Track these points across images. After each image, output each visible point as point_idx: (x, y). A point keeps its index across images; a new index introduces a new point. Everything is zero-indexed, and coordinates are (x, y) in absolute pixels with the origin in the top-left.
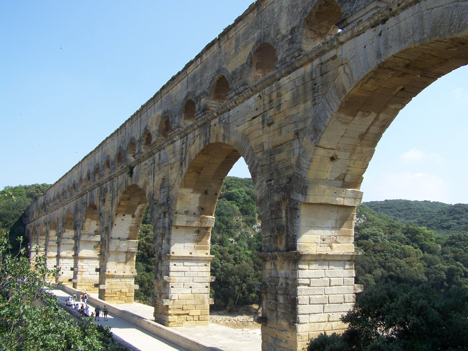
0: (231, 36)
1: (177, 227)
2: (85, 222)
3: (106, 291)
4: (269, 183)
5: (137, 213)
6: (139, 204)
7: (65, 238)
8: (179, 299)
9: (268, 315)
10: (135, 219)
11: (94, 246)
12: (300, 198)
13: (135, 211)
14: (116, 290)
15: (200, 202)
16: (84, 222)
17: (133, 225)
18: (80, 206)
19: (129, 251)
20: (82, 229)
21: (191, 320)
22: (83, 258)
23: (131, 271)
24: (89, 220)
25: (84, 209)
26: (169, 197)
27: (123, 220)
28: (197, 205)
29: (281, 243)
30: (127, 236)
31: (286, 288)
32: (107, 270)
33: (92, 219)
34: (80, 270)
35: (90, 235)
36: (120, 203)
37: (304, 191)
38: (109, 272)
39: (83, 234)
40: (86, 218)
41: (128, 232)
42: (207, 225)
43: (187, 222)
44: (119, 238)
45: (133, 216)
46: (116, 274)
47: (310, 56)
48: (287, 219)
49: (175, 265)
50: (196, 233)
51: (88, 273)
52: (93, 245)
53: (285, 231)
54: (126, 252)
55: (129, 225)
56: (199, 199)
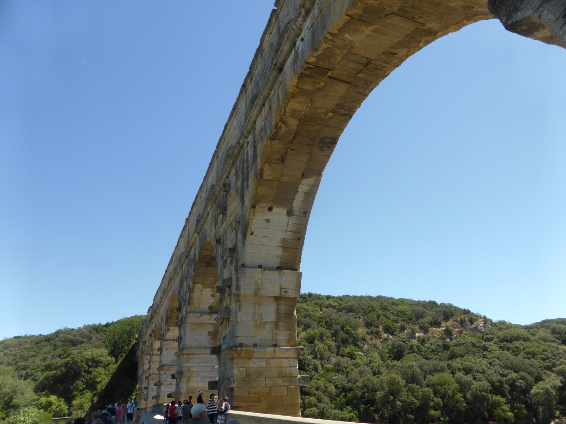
6: (303, 176)
7: (170, 340)
10: (293, 220)
11: (209, 333)
13: (293, 199)
19: (283, 294)
27: (268, 221)
30: (276, 263)
33: (205, 285)
35: (202, 313)
36: (262, 170)
39: (190, 312)
40: (194, 283)
41: (279, 252)
44: (260, 267)
45: (290, 213)
52: (207, 331)
54: (277, 299)
55: (282, 235)
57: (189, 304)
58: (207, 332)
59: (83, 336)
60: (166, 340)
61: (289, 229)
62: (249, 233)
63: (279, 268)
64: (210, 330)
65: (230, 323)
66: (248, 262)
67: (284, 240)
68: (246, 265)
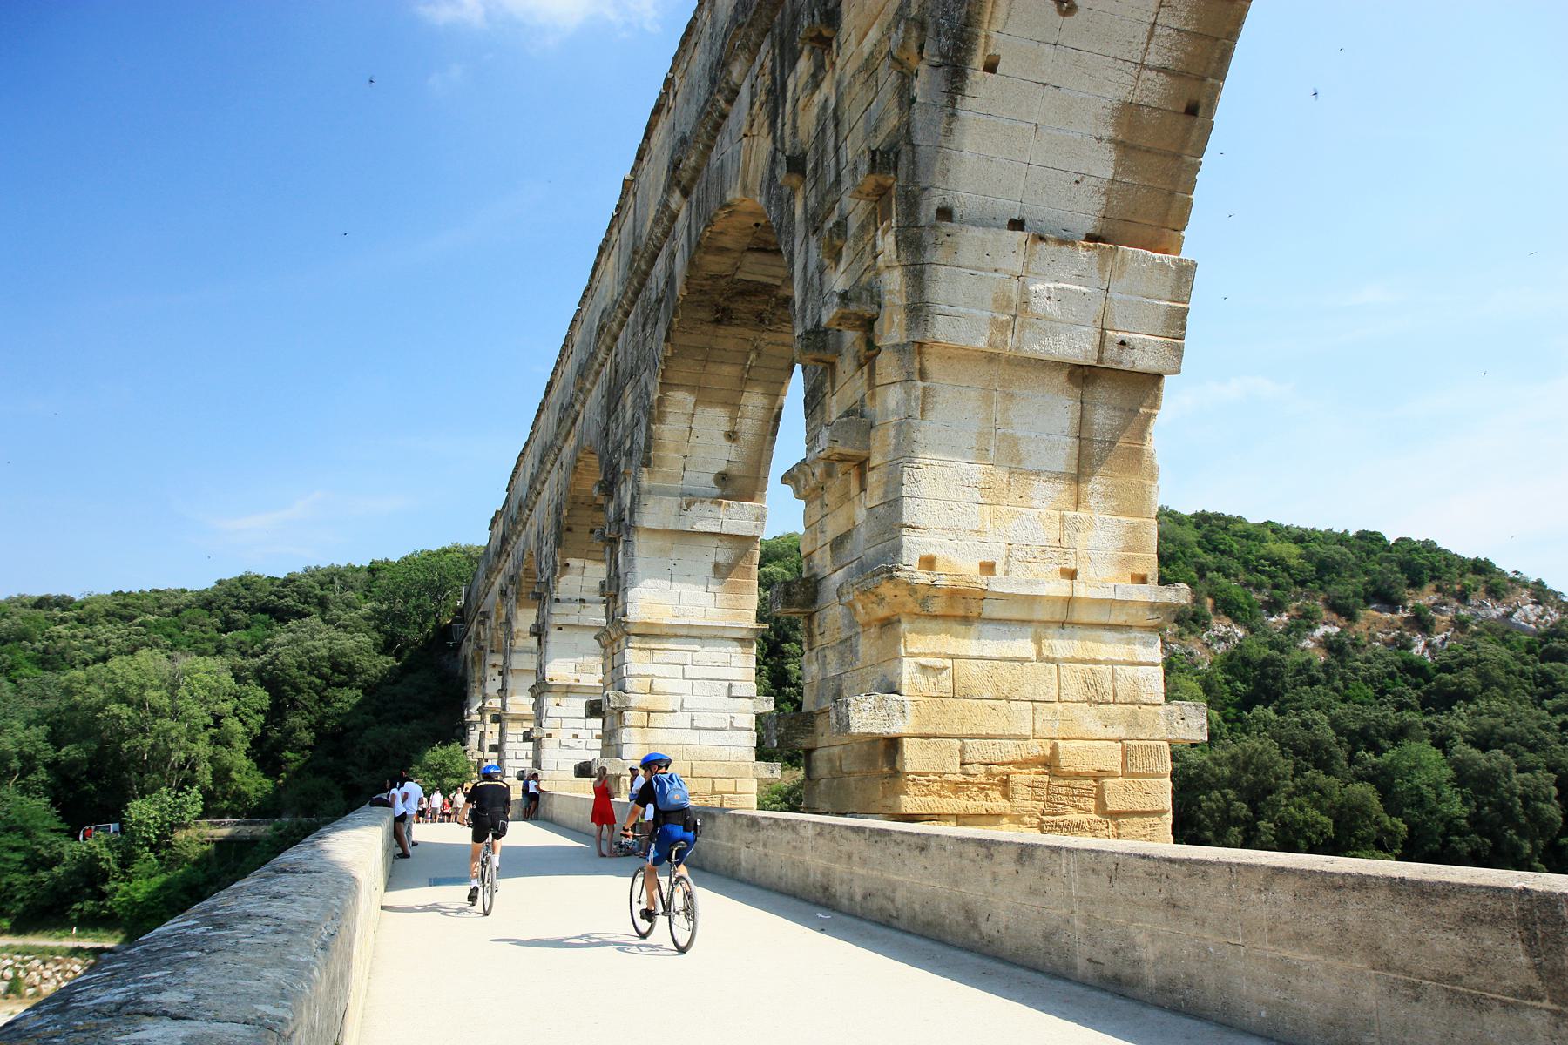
2: (661, 419)
3: (914, 757)
7: (570, 600)
11: (717, 566)
14: (1010, 751)
20: (647, 463)
22: (652, 634)
23: (1125, 562)
24: (682, 399)
32: (913, 548)
33: (704, 395)
34: (635, 701)
35: (690, 499)
38: (928, 563)
40: (666, 386)
41: (1103, 165)
44: (1016, 225)
46: (998, 584)
51: (683, 719)
54: (1083, 376)
55: (1118, 86)
58: (711, 566)
59: (305, 597)
60: (557, 600)
61: (1152, 59)
62: (978, 61)
64: (721, 559)
65: (872, 478)
67: (1128, 112)
68: (957, 213)
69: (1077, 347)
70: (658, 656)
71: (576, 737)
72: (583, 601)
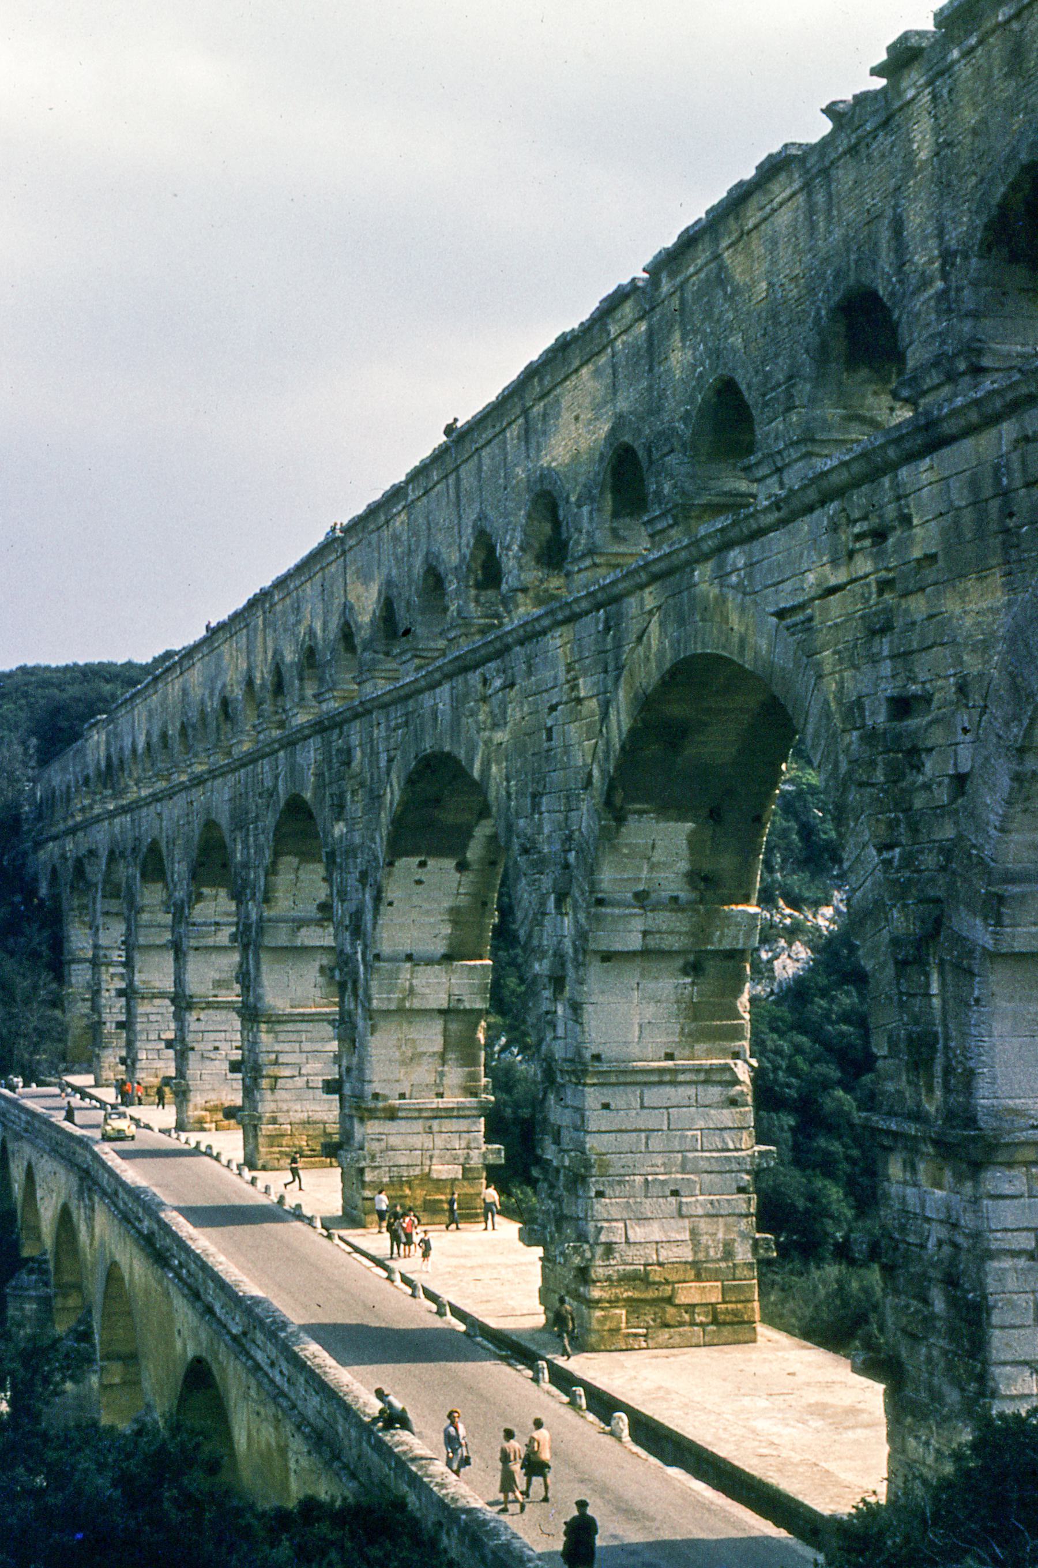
0: (750, 224)
1: (607, 957)
2: (275, 873)
4: (886, 855)
5: (474, 852)
8: (627, 1242)
9: (904, 1354)
10: (469, 877)
11: (322, 969)
12: (979, 932)
15: (691, 855)
16: (272, 870)
17: (463, 901)
18: (254, 804)
19: (453, 1004)
20: (267, 900)
21: (681, 1324)
22: (276, 1020)
25: (270, 820)
26: (569, 838)
27: (419, 882)
28: (683, 866)
29: (930, 1090)
30: (440, 948)
31: (953, 1261)
37: (994, 908)
40: (277, 854)
41: (447, 929)
42: (726, 945)
43: (645, 933)
44: (409, 957)
45: (462, 867)
47: (989, 409)
48: (944, 1002)
49: (606, 1106)
50: (686, 974)
52: (317, 965)
53: (940, 1046)
56: (689, 842)
57: (267, 900)
58: (317, 968)
61: (462, 891)
63: (448, 958)
64: (325, 962)
66: (385, 948)
69: (440, 1001)
70: (282, 1037)
71: (216, 1049)
72: (217, 924)
